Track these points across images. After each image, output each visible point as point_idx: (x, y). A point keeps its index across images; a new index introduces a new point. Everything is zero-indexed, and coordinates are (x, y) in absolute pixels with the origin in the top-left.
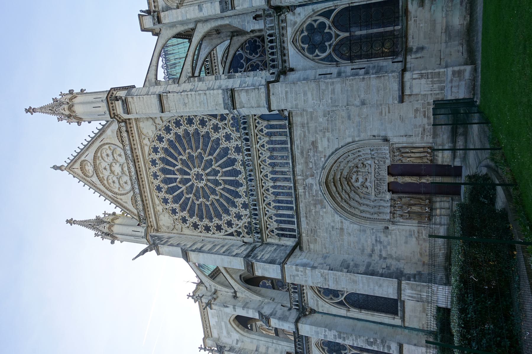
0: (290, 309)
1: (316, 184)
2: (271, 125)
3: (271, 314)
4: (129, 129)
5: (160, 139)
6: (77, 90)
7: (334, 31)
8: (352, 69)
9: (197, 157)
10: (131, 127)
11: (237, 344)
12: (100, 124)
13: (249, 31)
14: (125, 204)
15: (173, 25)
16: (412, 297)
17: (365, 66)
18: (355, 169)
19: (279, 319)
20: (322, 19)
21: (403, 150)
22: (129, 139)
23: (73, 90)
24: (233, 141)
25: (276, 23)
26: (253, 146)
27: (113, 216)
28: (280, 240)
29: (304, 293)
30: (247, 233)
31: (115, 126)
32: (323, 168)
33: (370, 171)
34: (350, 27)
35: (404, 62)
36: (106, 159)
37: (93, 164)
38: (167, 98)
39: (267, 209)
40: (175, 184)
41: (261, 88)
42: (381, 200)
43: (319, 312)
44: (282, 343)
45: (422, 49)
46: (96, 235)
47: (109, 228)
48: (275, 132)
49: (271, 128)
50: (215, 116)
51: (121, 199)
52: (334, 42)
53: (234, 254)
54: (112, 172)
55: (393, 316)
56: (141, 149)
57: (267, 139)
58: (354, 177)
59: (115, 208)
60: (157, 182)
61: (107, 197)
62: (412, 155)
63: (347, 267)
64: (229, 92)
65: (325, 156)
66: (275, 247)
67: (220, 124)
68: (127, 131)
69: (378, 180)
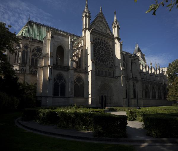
60: (100, 39)
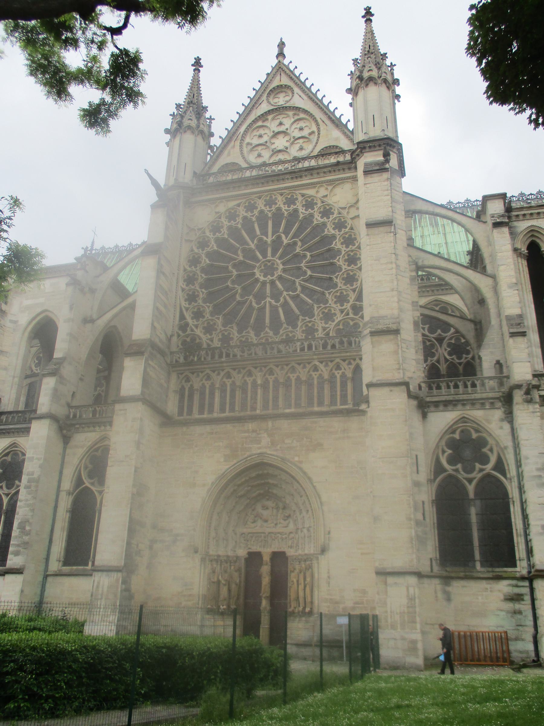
0: (69, 406)
1: (259, 448)
2: (346, 382)
3: (61, 377)
4: (340, 167)
5: (326, 212)
6: (398, 90)
7: (477, 476)
8: (423, 502)
9: (299, 268)
10: (344, 169)
11: (11, 321)
12: (349, 121)
13: (480, 354)
14: (226, 152)
15: (490, 243)
16: (98, 587)
17: (428, 520)
18: (281, 505)
19: (55, 390)
20: (493, 459)
21: (308, 574)
22: (325, 167)
23: (398, 85)
24: (324, 325)
25: (491, 395)
26: (316, 355)
27: (207, 133)
28: (175, 391)
29: (94, 427)
30: (185, 341)
31: (345, 144)
32: (283, 460)
33: (279, 525)
34: (481, 499)
35: (432, 574)
36: (295, 126)
37: (287, 105)
38: (387, 233)
39: (222, 374)
40: (258, 232)
41: (399, 373)
42: (236, 542)
43: (65, 449)
44: (14, 391)
45: (449, 599)
46: (178, 106)
47: (189, 127)
48: (335, 387)
49: (342, 382)
50: (360, 298)
51: (234, 147)
52: (462, 476)
53: (156, 324)
54: (276, 135)
55: (62, 559)
56: (312, 184)
57: (326, 376)
58: (270, 504)
59: (220, 137)
60: (261, 205)
61: (237, 125)
62: (301, 587)
63: (138, 494)
64: (394, 327)
65: (301, 462)
66: (165, 385)
67: (347, 306)
68: (338, 163)
69: (265, 537)
